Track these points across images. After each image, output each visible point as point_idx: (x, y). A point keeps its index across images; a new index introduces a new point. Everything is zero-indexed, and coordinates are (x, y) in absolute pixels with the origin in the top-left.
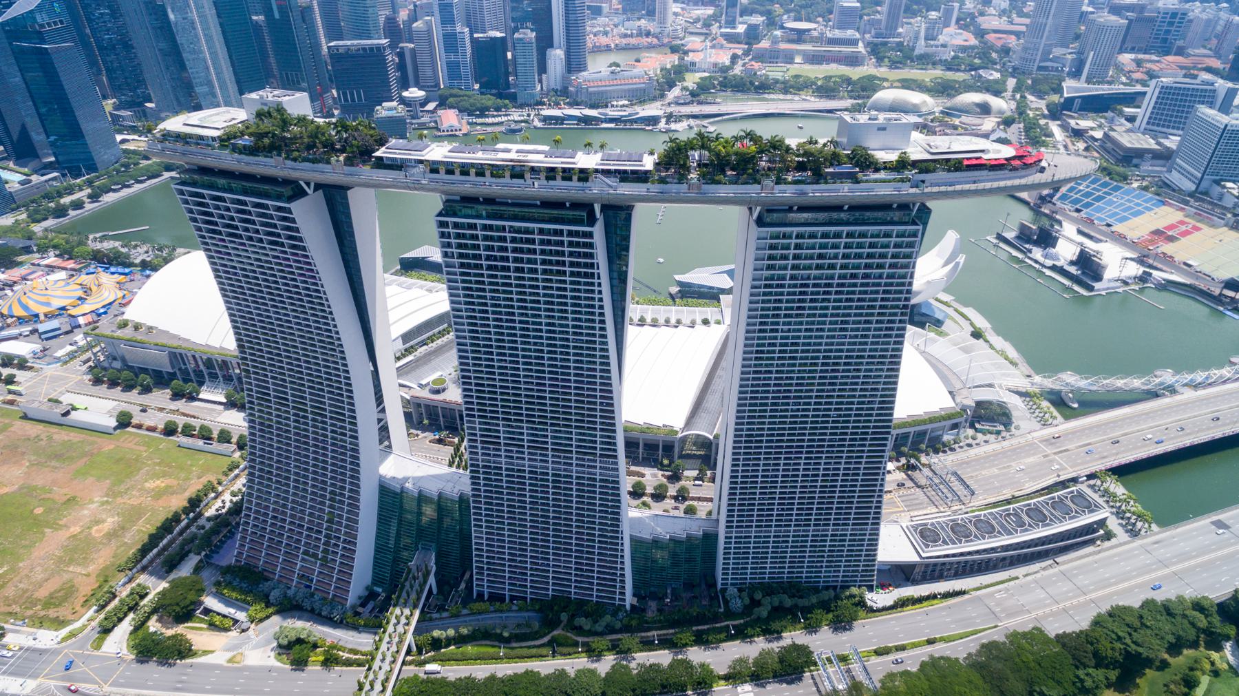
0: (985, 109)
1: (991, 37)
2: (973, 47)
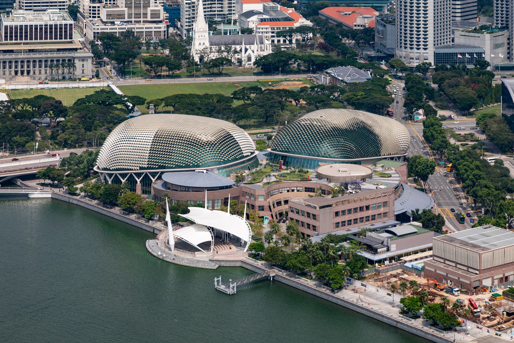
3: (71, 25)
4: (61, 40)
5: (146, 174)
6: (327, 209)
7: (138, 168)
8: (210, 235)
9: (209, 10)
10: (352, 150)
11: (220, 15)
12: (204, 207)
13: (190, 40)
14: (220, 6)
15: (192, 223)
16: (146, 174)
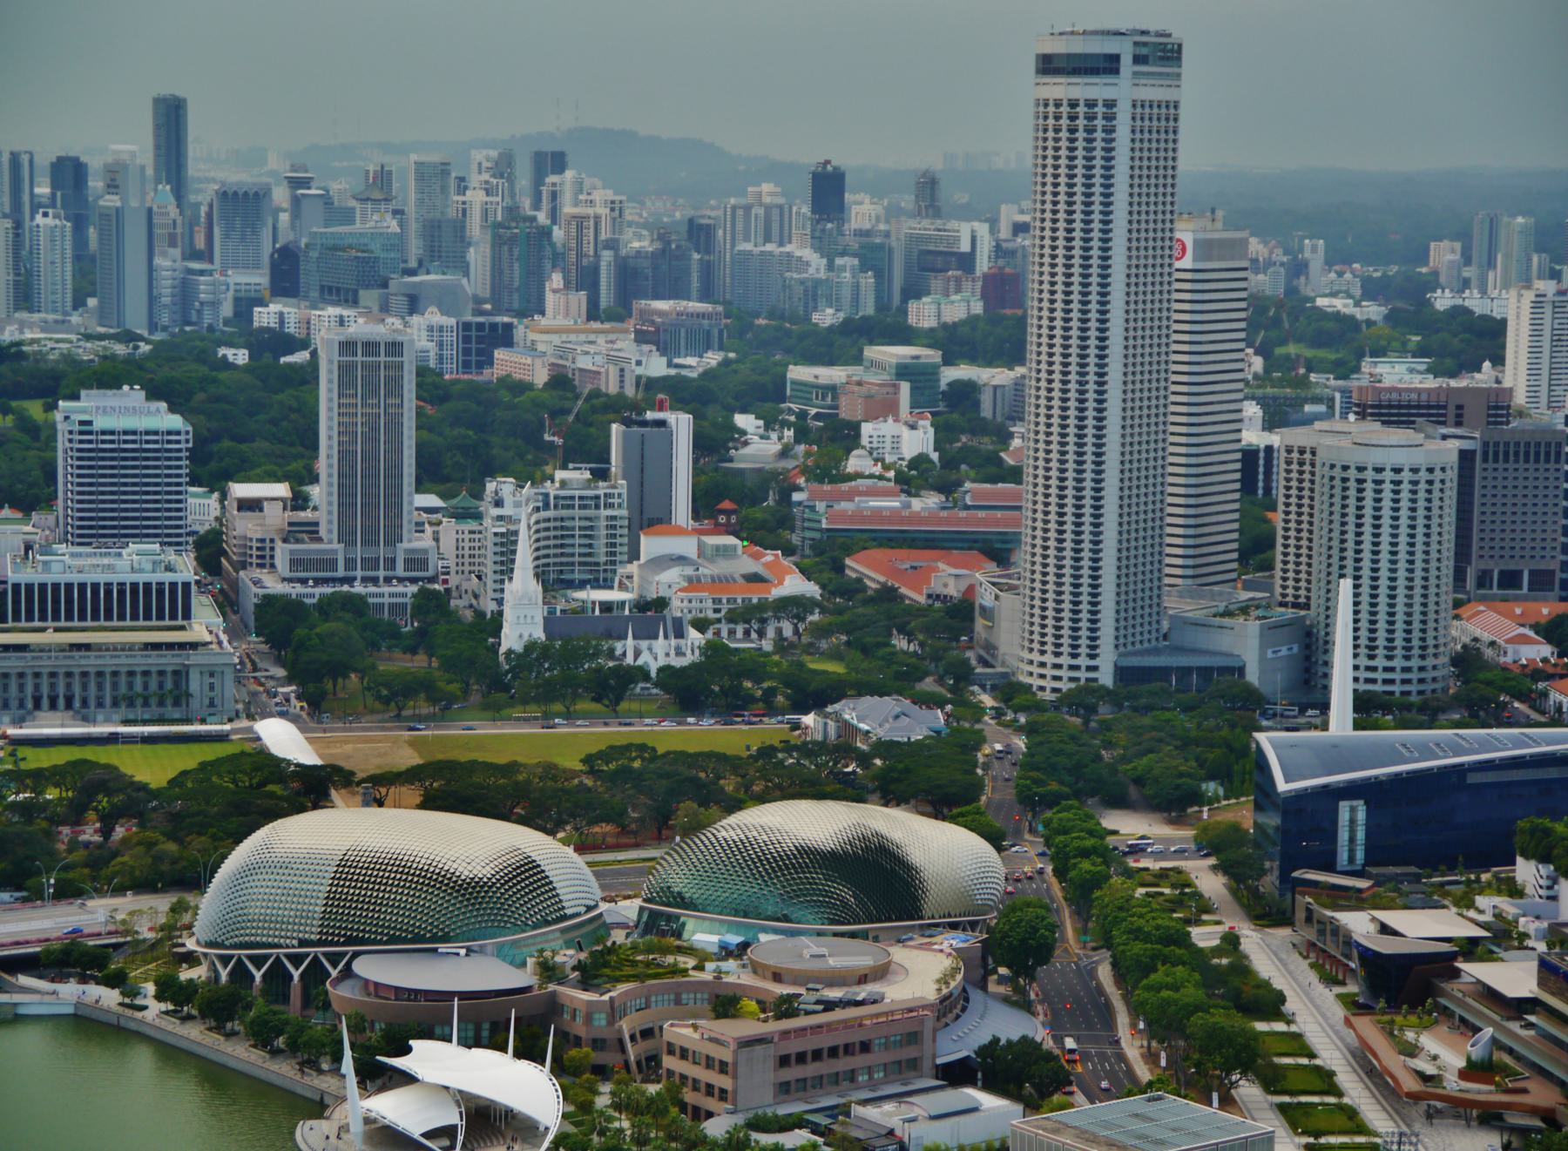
0: (877, 889)
1: (864, 569)
2: (794, 607)
3: (186, 585)
4: (173, 623)
5: (316, 958)
6: (758, 1048)
7: (295, 942)
8: (457, 1111)
9: (559, 551)
10: (845, 904)
11: (585, 564)
12: (450, 1041)
13: (495, 625)
14: (587, 541)
15: (408, 1079)
16: (316, 958)
